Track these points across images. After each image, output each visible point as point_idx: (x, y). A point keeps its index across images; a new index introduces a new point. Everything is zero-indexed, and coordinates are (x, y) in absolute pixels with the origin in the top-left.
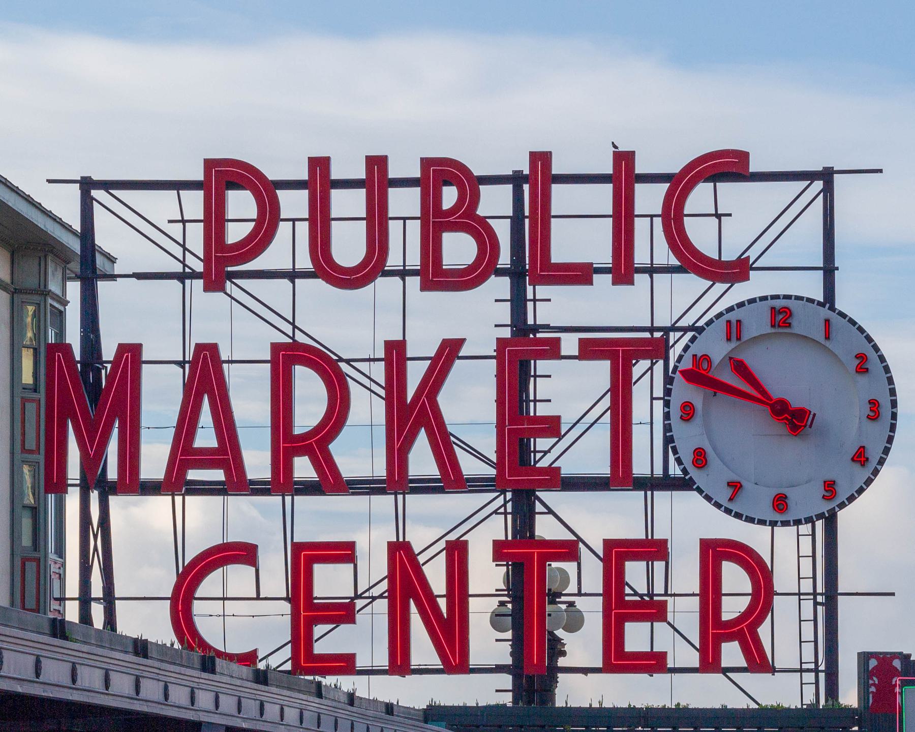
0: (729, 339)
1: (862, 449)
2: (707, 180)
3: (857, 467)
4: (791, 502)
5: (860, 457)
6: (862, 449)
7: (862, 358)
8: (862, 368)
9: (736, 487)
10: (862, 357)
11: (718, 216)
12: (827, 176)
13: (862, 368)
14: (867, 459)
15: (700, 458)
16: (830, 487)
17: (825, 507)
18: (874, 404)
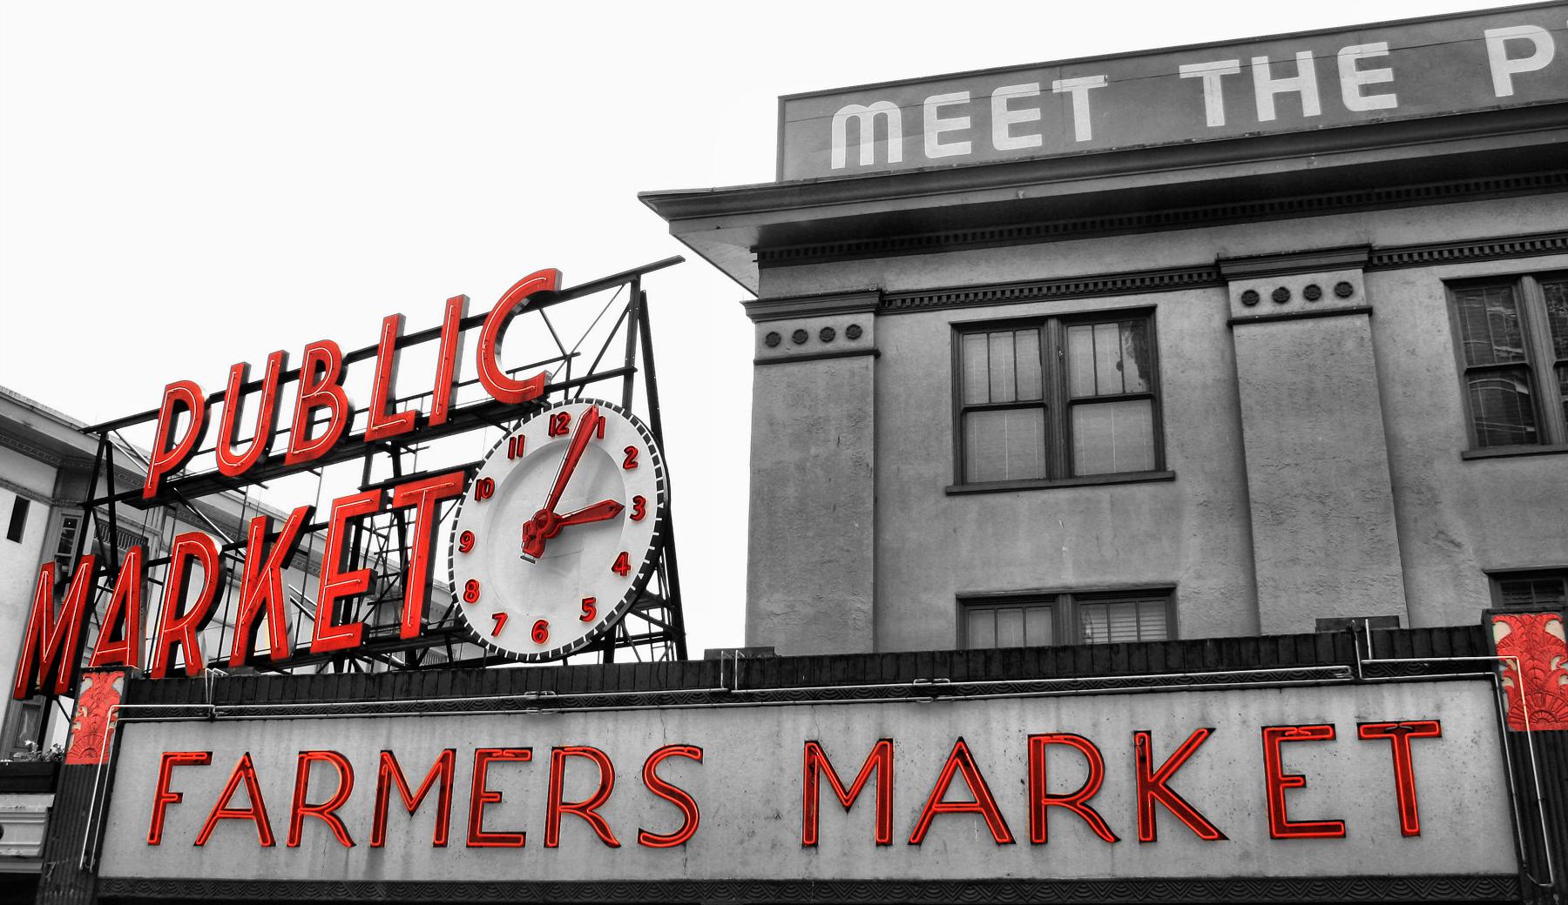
0: (511, 456)
1: (624, 555)
2: (525, 309)
3: (615, 578)
4: (551, 631)
5: (621, 566)
6: (624, 555)
7: (631, 452)
8: (631, 461)
9: (500, 619)
10: (631, 452)
11: (568, 358)
12: (633, 277)
13: (631, 461)
14: (628, 567)
15: (472, 590)
16: (589, 605)
17: (582, 631)
18: (639, 502)
